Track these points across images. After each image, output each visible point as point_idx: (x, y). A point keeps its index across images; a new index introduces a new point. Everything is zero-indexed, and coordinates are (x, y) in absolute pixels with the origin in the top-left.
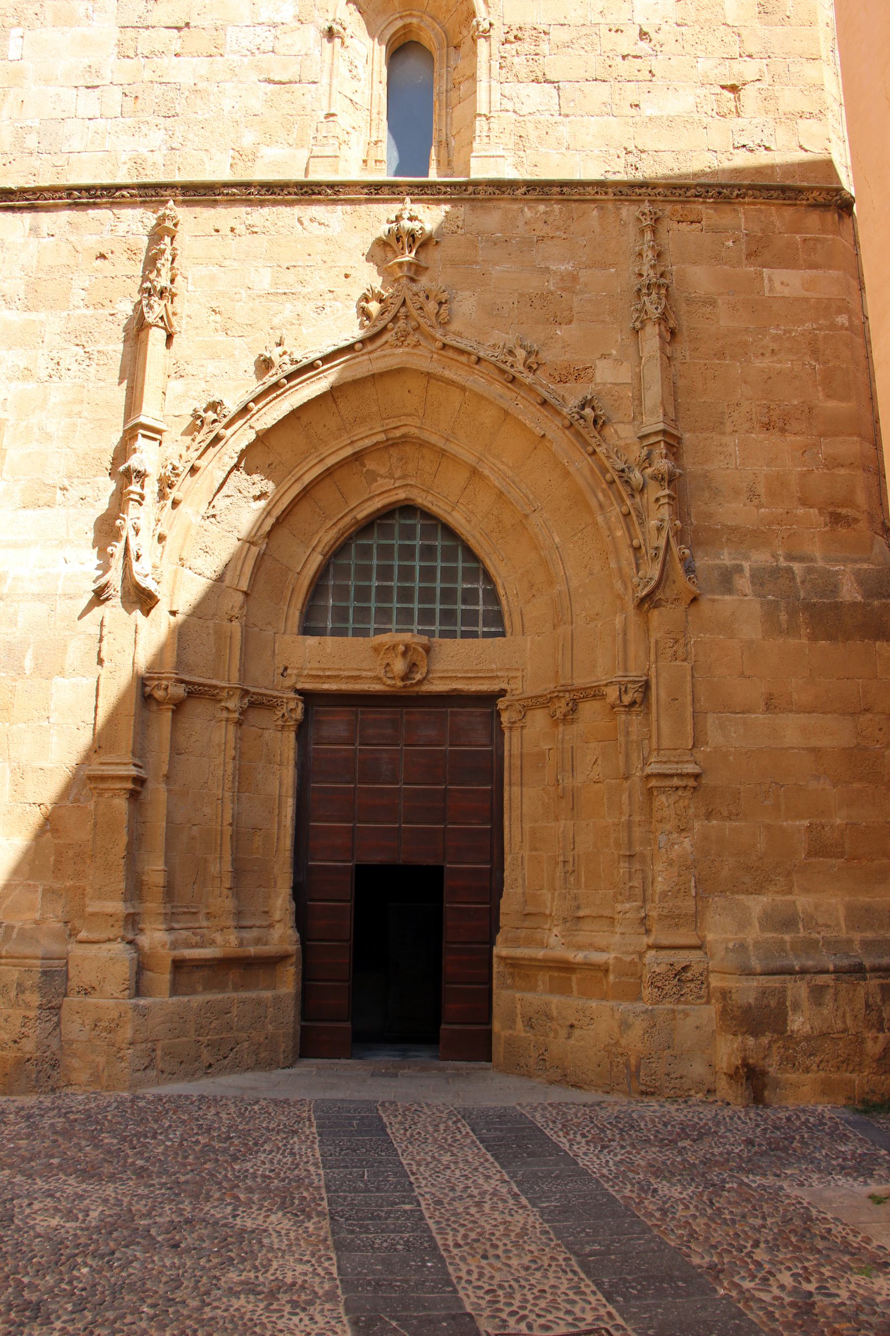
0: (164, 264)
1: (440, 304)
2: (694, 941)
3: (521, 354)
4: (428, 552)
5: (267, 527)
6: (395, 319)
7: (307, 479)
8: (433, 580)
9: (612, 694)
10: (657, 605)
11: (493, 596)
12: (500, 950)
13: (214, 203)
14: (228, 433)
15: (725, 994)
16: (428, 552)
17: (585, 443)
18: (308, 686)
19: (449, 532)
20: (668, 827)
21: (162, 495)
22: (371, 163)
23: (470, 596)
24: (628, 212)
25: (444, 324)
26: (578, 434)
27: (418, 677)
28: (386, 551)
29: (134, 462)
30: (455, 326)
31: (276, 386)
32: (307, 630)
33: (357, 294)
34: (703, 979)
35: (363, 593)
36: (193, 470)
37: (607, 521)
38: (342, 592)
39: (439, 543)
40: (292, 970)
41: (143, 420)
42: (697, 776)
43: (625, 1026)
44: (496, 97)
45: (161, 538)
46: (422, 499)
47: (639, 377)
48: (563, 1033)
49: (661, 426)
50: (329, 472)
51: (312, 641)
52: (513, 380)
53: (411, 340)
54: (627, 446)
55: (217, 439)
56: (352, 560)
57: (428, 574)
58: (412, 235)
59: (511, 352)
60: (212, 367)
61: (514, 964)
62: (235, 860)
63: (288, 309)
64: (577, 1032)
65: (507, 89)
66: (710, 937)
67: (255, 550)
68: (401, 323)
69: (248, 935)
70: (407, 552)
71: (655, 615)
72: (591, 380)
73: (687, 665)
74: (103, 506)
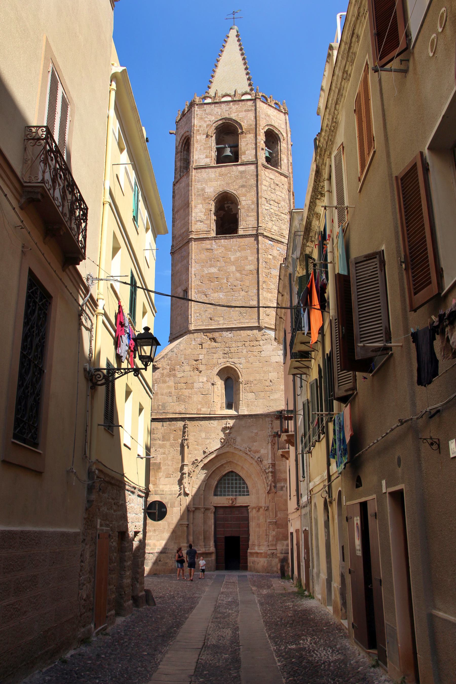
0: (186, 434)
1: (234, 440)
2: (275, 549)
3: (248, 449)
4: (236, 480)
5: (207, 479)
6: (226, 443)
7: (213, 470)
8: (237, 485)
9: (263, 508)
10: (270, 493)
11: (247, 487)
12: (249, 551)
13: (194, 421)
14: (199, 464)
15: (279, 557)
16: (236, 480)
17: (259, 465)
18: (215, 505)
19: (239, 476)
20: (271, 530)
21: (189, 476)
22: (222, 407)
23: (244, 488)
24: (267, 419)
25: (235, 444)
26: (257, 463)
27: (234, 503)
28: (228, 480)
29: (184, 471)
30: (237, 444)
31: (207, 456)
32: (215, 495)
33: (220, 438)
34: (276, 555)
35: (225, 488)
36: (194, 471)
37: (263, 478)
38: (221, 488)
39: (238, 478)
40: (214, 555)
41: (185, 463)
42: (276, 522)
43: (264, 562)
44: (244, 396)
45: (189, 483)
46: (234, 470)
47: (268, 452)
48: (257, 564)
49: (270, 462)
50: (217, 468)
51: (216, 497)
52: (247, 454)
53: (229, 446)
54: (266, 465)
55: (197, 466)
56: (223, 481)
57: (236, 484)
58: (229, 427)
59: (246, 449)
60: (196, 452)
61: (251, 553)
62: (204, 536)
63: (208, 441)
64: (259, 564)
65: (246, 394)
66: (278, 548)
67: (205, 483)
68: (227, 444)
69: (207, 549)
70: (232, 480)
71: (269, 495)
72: (260, 453)
73: (274, 504)
74: (179, 477)
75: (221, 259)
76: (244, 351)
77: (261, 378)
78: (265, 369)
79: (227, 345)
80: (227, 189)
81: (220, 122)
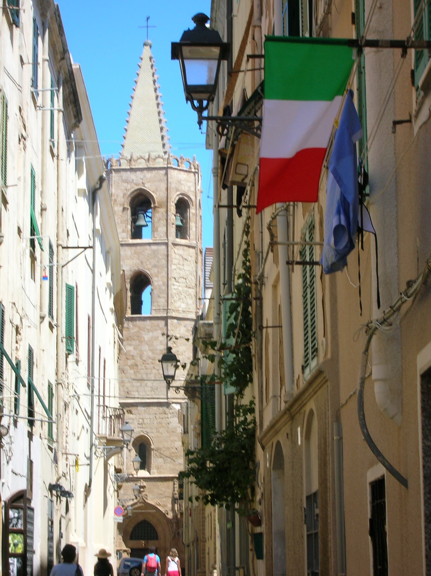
75: (135, 338)
76: (155, 423)
77: (169, 446)
78: (172, 438)
79: (141, 417)
80: (141, 268)
81: (135, 193)
